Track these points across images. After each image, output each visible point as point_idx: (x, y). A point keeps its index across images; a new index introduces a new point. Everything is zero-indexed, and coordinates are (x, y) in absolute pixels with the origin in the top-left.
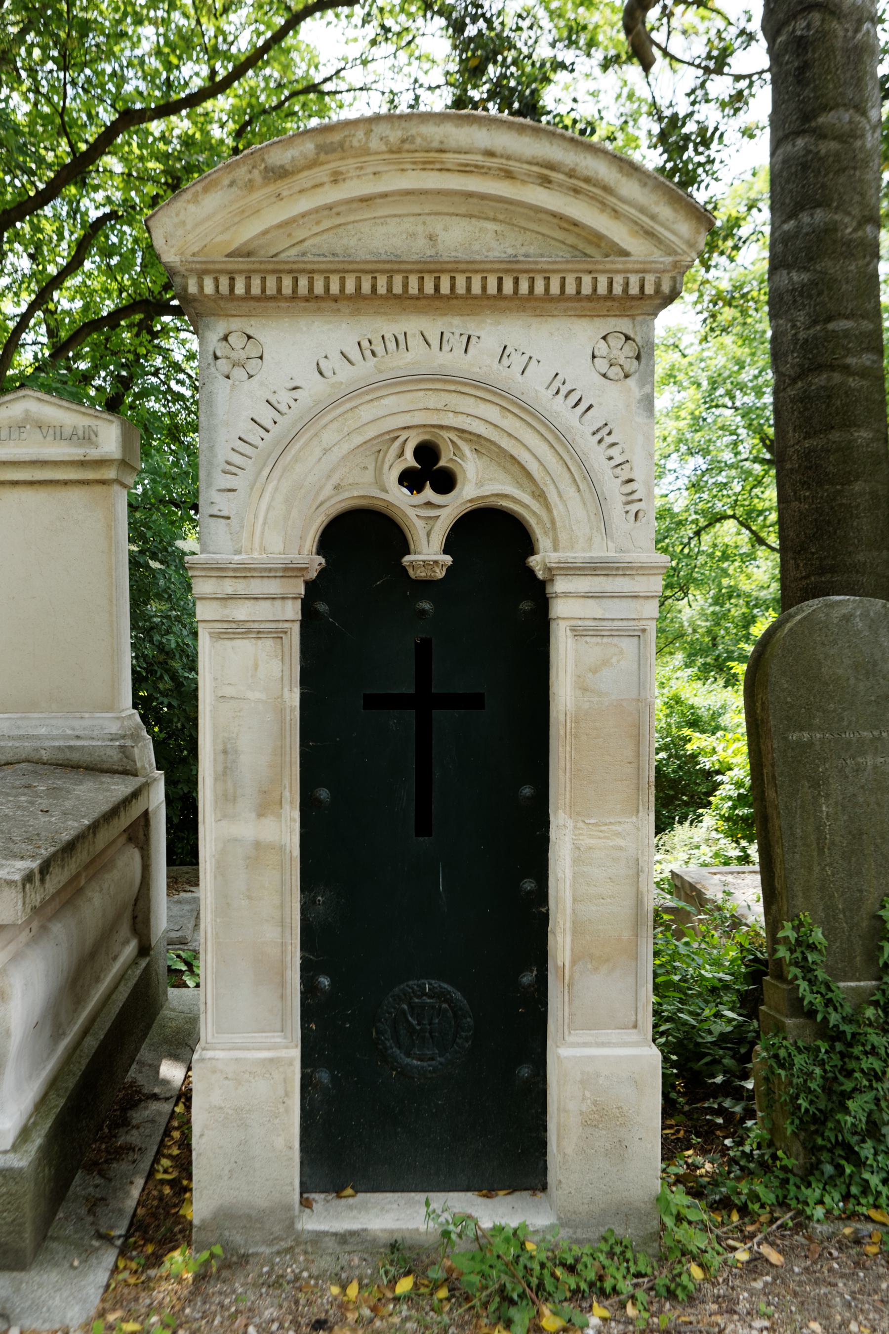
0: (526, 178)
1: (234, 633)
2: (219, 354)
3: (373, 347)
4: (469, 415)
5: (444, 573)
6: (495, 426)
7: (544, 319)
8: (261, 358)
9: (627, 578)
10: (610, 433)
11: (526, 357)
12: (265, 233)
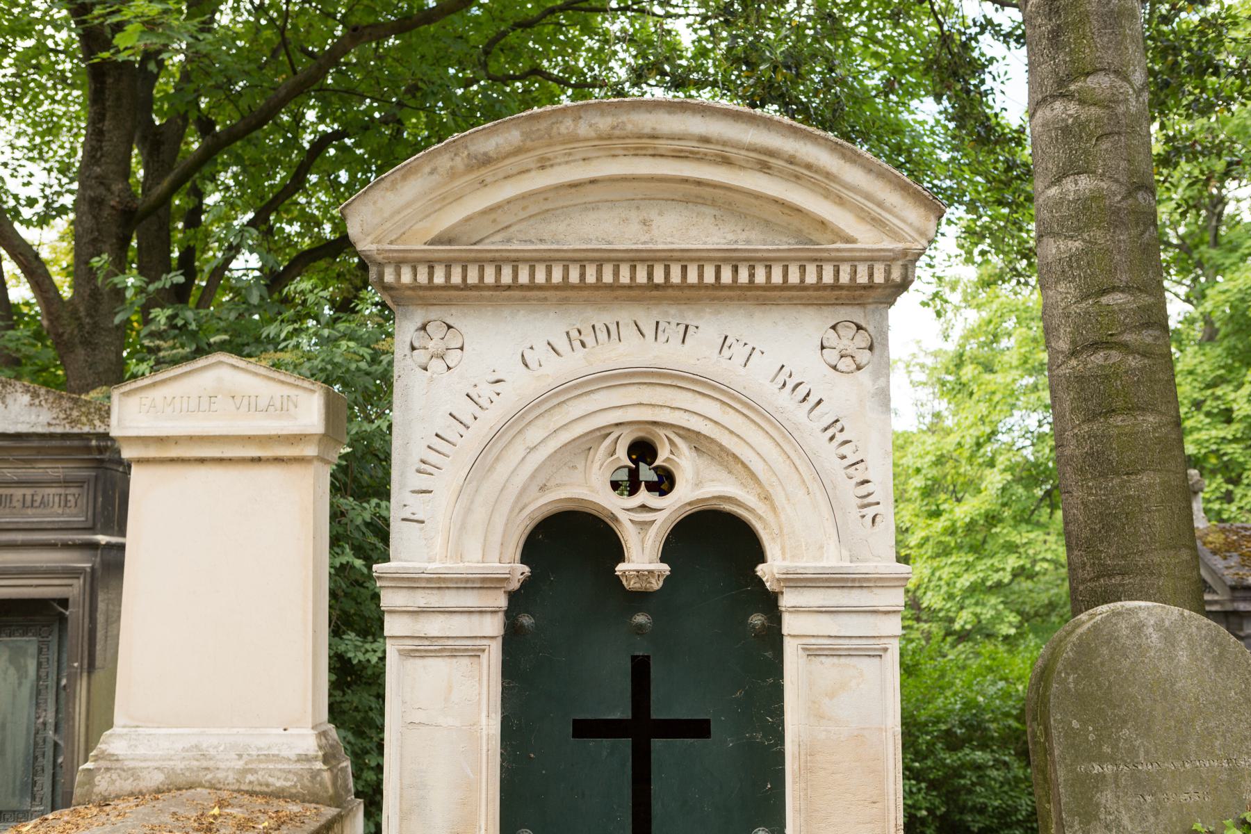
0: (743, 164)
1: (426, 651)
2: (416, 344)
3: (582, 338)
4: (686, 411)
5: (661, 584)
6: (716, 422)
7: (768, 307)
8: (462, 349)
9: (865, 591)
10: (842, 430)
11: (748, 348)
12: (468, 219)
